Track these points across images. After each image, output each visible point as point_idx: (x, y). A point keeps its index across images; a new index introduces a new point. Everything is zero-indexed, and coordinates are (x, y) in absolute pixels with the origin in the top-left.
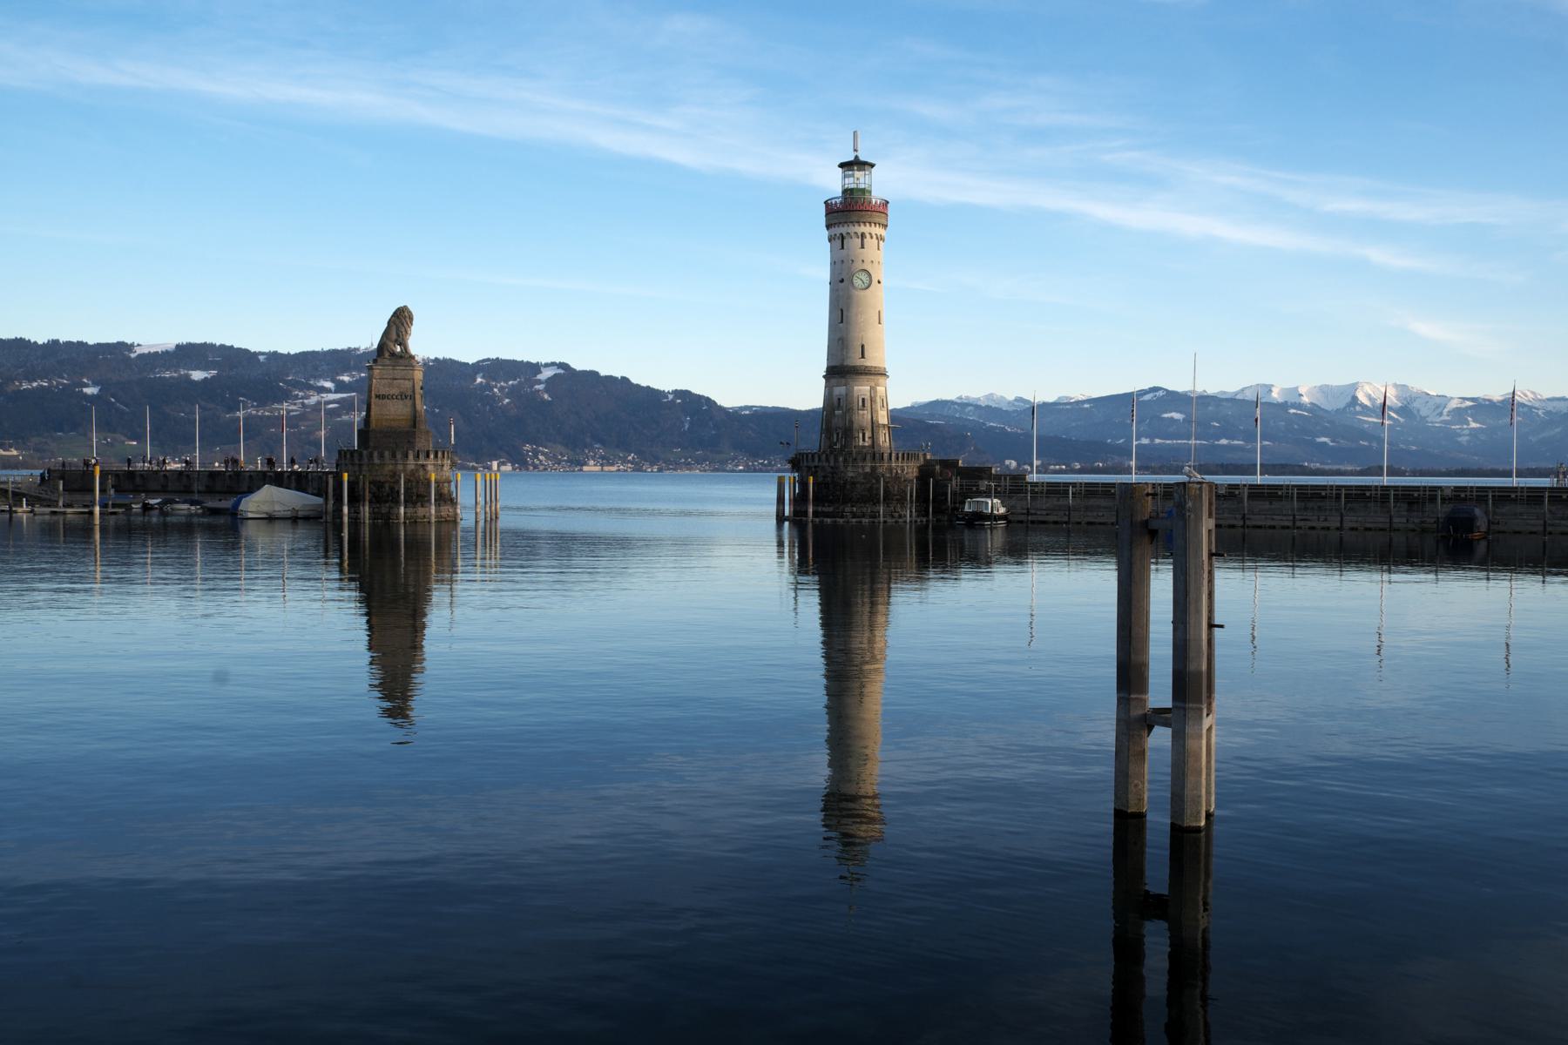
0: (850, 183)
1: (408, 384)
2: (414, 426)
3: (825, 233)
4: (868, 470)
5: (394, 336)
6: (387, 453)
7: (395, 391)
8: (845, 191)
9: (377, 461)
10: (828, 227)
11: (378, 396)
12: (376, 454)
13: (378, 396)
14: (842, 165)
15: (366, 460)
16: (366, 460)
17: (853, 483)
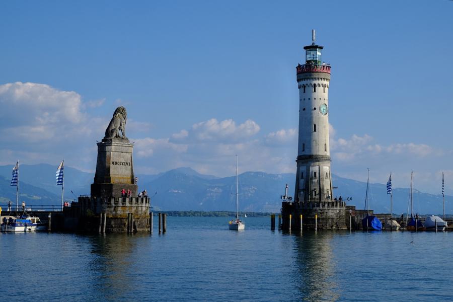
0: (309, 58)
1: (128, 156)
2: (133, 181)
3: (297, 84)
4: (338, 212)
5: (119, 126)
6: (134, 199)
7: (122, 160)
8: (308, 62)
9: (127, 204)
10: (298, 81)
11: (113, 163)
12: (127, 200)
13: (113, 163)
14: (305, 48)
15: (120, 204)
16: (120, 204)
17: (333, 219)
